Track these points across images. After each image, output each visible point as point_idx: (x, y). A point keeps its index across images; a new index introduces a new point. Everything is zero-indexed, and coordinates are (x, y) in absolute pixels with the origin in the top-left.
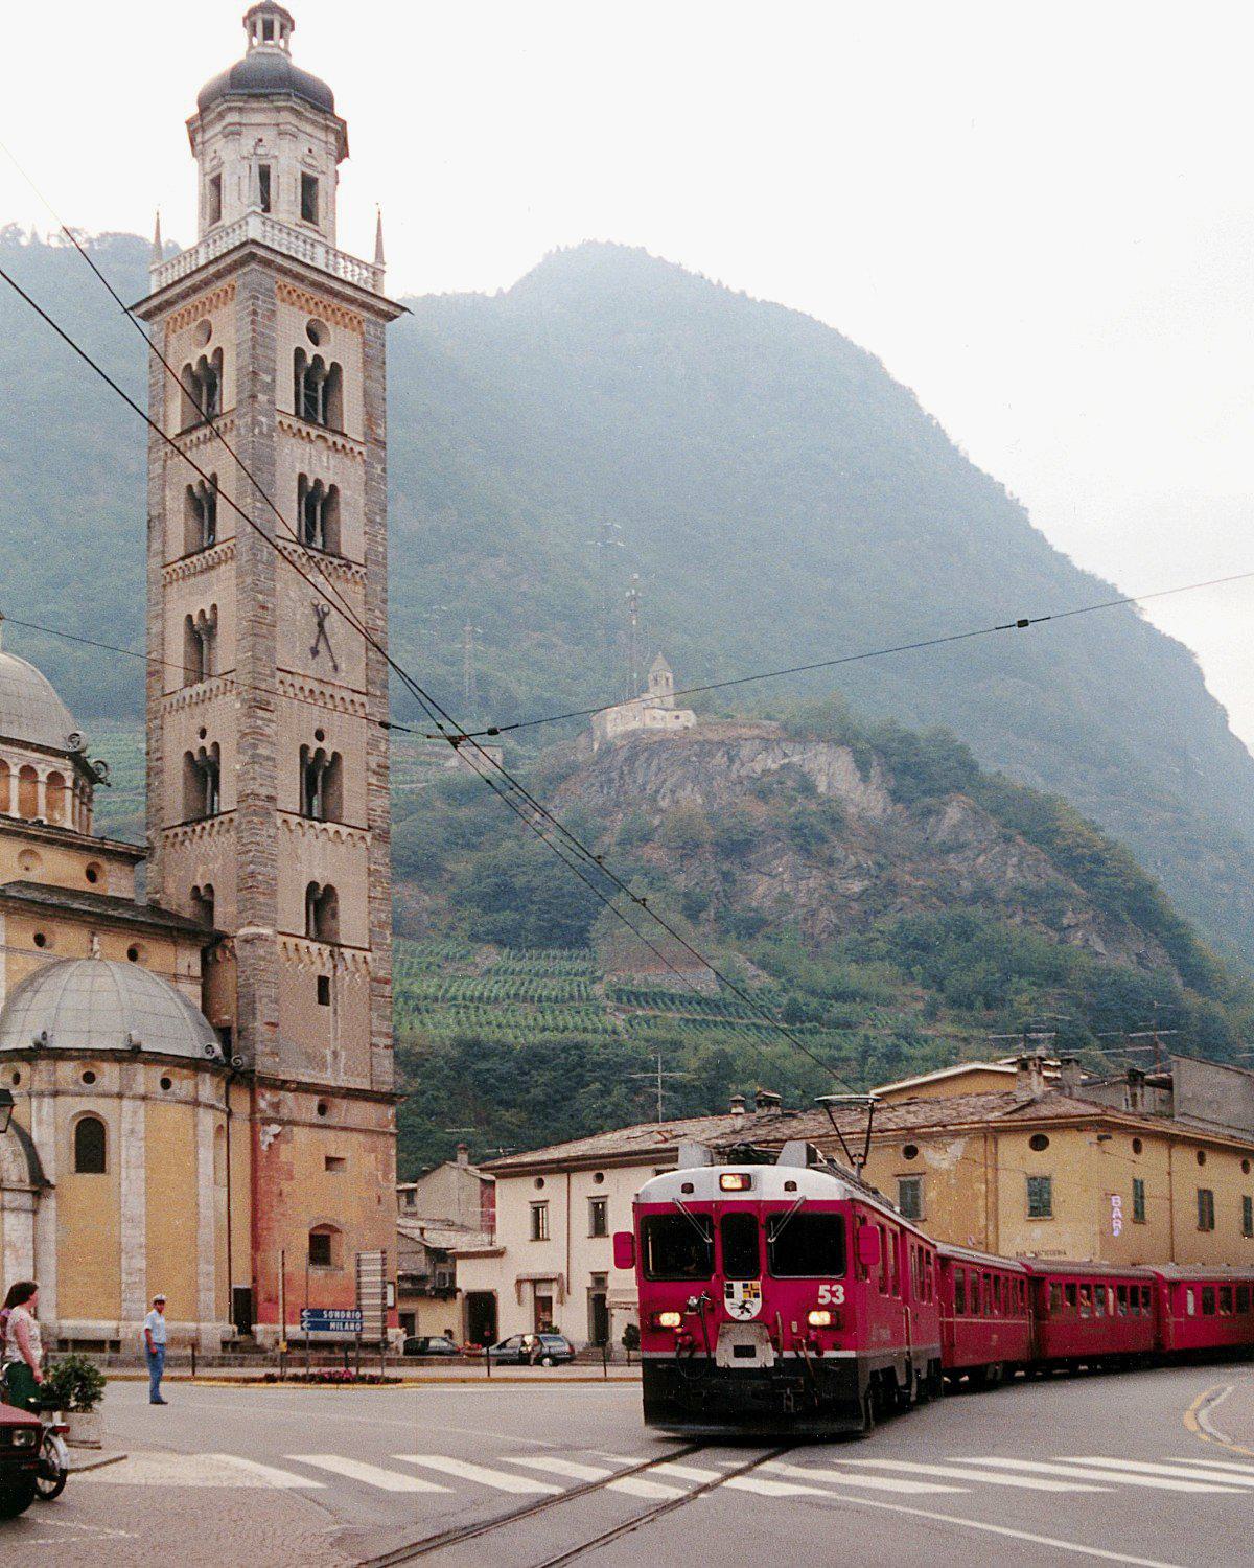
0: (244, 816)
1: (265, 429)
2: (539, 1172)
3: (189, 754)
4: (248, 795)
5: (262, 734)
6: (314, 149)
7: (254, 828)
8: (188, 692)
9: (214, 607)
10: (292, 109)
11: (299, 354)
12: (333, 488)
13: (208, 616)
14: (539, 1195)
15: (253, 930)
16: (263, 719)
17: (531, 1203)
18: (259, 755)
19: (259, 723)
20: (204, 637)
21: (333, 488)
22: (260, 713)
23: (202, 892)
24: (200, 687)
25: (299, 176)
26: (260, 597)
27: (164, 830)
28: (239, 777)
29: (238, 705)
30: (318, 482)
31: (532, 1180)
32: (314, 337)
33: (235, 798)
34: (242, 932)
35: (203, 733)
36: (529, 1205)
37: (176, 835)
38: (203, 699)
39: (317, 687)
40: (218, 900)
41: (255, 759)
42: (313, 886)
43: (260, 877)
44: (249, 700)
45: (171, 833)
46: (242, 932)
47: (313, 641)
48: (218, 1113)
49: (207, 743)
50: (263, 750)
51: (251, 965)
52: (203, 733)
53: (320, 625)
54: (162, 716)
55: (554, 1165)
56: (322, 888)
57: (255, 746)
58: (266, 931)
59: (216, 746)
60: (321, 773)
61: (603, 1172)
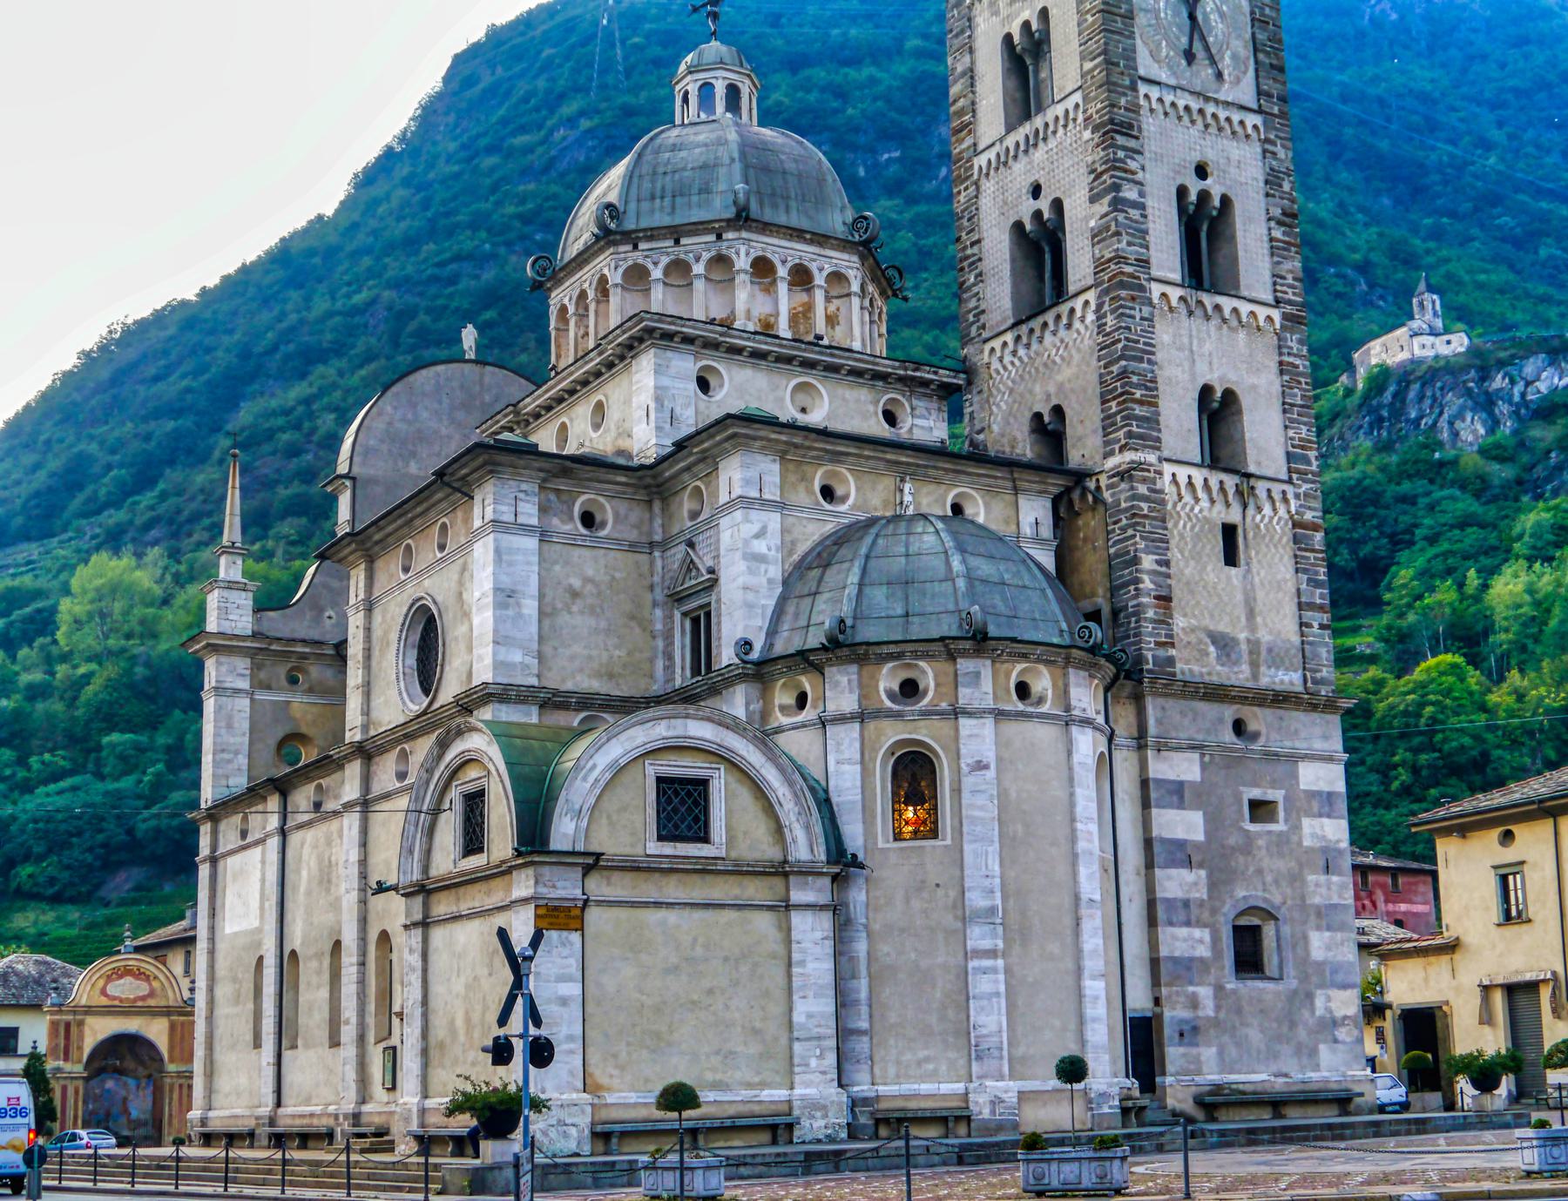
0: (1106, 292)
2: (1505, 822)
3: (1018, 226)
4: (1110, 260)
5: (1126, 171)
7: (1121, 306)
8: (1010, 142)
9: (1044, 14)
13: (1034, 27)
14: (1509, 855)
15: (1129, 456)
16: (1124, 148)
17: (1495, 867)
18: (1125, 201)
19: (1121, 154)
20: (1028, 61)
22: (1121, 140)
23: (1047, 419)
24: (1026, 129)
27: (986, 341)
28: (1098, 236)
29: (1087, 135)
31: (1495, 833)
33: (1091, 270)
34: (1111, 463)
35: (1036, 191)
36: (1493, 872)
37: (1005, 344)
38: (1031, 144)
39: (1195, 105)
40: (1072, 430)
41: (1118, 204)
42: (1206, 391)
43: (1135, 379)
44: (1103, 125)
45: (997, 343)
46: (1111, 463)
47: (1184, 40)
48: (1098, 734)
49: (1044, 204)
50: (1130, 193)
51: (1126, 510)
52: (1036, 191)
53: (1192, 17)
54: (976, 183)
55: (1535, 806)
56: (1219, 394)
57: (1116, 188)
58: (1152, 458)
59: (1058, 205)
60: (1205, 227)
61: (1513, 828)
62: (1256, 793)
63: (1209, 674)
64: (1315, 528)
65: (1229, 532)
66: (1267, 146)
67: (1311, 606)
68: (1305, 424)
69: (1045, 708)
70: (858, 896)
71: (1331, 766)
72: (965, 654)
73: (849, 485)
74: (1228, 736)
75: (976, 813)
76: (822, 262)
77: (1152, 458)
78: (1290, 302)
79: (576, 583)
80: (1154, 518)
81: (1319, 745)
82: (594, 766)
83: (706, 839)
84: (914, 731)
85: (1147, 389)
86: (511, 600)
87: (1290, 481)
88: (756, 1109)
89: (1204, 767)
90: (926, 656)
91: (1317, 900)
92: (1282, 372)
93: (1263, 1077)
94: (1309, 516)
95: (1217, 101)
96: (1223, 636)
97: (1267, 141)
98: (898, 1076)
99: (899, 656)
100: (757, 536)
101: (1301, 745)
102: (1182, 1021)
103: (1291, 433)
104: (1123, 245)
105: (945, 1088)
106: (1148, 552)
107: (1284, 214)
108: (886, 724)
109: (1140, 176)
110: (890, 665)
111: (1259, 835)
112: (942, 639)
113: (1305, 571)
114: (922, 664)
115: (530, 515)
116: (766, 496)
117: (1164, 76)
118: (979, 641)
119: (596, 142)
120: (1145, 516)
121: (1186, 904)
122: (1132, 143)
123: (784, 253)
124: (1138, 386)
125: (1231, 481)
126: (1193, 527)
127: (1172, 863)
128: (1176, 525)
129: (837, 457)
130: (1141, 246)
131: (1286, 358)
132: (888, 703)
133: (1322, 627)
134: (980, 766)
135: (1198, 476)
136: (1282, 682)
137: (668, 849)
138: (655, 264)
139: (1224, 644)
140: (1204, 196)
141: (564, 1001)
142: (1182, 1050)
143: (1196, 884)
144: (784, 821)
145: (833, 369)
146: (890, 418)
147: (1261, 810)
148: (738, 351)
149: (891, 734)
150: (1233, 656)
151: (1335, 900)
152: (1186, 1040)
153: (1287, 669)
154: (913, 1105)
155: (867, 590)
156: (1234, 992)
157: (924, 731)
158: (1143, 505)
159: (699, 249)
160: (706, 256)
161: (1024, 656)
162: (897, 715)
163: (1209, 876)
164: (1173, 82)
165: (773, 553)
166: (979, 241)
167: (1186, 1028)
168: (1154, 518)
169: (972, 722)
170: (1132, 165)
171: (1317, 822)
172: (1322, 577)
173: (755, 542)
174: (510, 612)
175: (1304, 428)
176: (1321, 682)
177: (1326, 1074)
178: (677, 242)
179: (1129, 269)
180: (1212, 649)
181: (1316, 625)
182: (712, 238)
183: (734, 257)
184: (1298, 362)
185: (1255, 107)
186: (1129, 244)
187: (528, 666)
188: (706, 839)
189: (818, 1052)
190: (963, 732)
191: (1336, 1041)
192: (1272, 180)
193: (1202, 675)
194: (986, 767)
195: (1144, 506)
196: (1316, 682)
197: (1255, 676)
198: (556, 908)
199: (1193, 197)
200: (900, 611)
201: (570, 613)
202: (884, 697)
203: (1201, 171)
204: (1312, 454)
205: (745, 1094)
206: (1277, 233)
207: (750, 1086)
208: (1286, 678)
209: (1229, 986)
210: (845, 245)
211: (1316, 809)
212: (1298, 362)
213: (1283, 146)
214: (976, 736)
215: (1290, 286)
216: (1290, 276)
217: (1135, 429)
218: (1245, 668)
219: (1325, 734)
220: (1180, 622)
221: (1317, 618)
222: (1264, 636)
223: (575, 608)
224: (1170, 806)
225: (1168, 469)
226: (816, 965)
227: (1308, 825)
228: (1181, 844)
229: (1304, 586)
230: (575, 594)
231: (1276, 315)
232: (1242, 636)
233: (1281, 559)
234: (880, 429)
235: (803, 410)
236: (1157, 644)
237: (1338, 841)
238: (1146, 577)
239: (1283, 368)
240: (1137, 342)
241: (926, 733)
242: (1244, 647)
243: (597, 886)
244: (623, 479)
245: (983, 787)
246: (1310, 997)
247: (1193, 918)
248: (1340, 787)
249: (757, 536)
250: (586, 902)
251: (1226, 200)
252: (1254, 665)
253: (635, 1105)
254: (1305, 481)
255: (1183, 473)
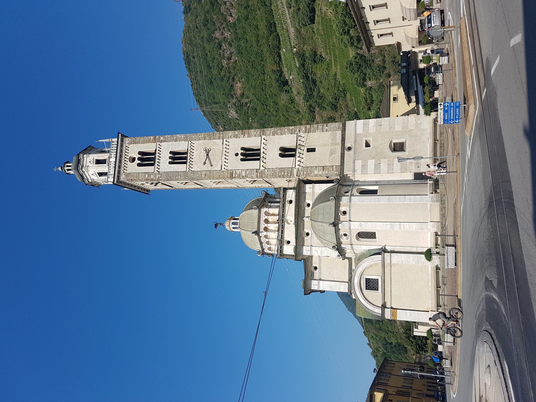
1: (160, 176)
6: (89, 161)
10: (81, 169)
11: (139, 165)
12: (171, 153)
16: (235, 175)
19: (236, 176)
21: (171, 153)
22: (234, 176)
25: (97, 165)
26: (203, 176)
30: (170, 158)
32: (133, 160)
42: (281, 156)
43: (280, 174)
57: (243, 177)
62: (364, 145)
63: (338, 157)
64: (306, 128)
65: (309, 150)
66: (230, 137)
67: (323, 129)
68: (285, 130)
69: (348, 209)
70: (388, 248)
71: (357, 124)
72: (338, 227)
73: (306, 231)
74: (352, 152)
75: (370, 226)
76: (263, 217)
77: (295, 171)
78: (260, 133)
79: (328, 273)
80: (307, 170)
81: (353, 128)
82: (364, 304)
83: (378, 280)
84: (354, 236)
85: (281, 171)
86: (332, 287)
87: (297, 134)
88: (433, 274)
89: (359, 160)
90: (339, 234)
91: (388, 128)
92: (274, 135)
93: (429, 144)
94: (304, 129)
95: (222, 151)
96: (330, 153)
97: (228, 138)
98: (426, 243)
99: (339, 238)
100: (317, 252)
101: (353, 133)
102: (415, 165)
103: (287, 134)
104: (254, 176)
105: (429, 235)
106: (314, 172)
107: (242, 134)
108: (352, 241)
109: (240, 171)
110: (341, 239)
111: (373, 144)
112: (335, 233)
113: (315, 131)
114: (340, 234)
115: (316, 282)
116: (310, 250)
117: (220, 163)
118: (335, 224)
119: (231, 110)
120: (307, 173)
121: (389, 165)
122: (234, 172)
123: (263, 225)
124: (281, 174)
125: (298, 151)
126: (308, 160)
127: (380, 168)
128: (308, 165)
129: (301, 234)
130: (254, 171)
131: (272, 134)
132: (349, 240)
133: (327, 126)
134: (361, 225)
135: (298, 159)
136: (339, 137)
137: (380, 288)
138: (267, 246)
139: (332, 153)
140: (242, 154)
141: (411, 315)
142: (422, 167)
143: (384, 162)
144: (373, 263)
145: (283, 215)
146: (291, 202)
147: (367, 145)
148: (282, 236)
149: (354, 240)
150: (334, 150)
151: (388, 123)
152: (419, 166)
153: (336, 135)
154: (433, 241)
155: (326, 239)
156: (409, 152)
157: (354, 234)
158: (305, 173)
159: (263, 240)
160: (265, 239)
161: (338, 214)
162: (351, 239)
163: (382, 158)
164: (220, 161)
165: (320, 249)
166: (255, 186)
167: (417, 166)
168: (307, 170)
169: (352, 226)
170: (238, 173)
171: (370, 129)
172: (316, 126)
173: (318, 253)
174: (334, 287)
175: (286, 130)
176: (339, 126)
177: (428, 127)
178: (263, 243)
179: (258, 174)
180: (333, 156)
181: (327, 128)
182: (261, 238)
183: (264, 235)
184: (272, 131)
185: (222, 140)
186: (254, 174)
187: (344, 285)
188: (378, 280)
189: (421, 259)
190: (354, 228)
191: (421, 123)
192: (236, 136)
193: (339, 158)
194: (361, 224)
195: (305, 173)
196: (339, 128)
197: (339, 144)
198: (393, 315)
199: (242, 157)
200: (330, 235)
201: (333, 274)
202: (347, 240)
203: (237, 155)
204: (291, 128)
205: (430, 276)
206: (247, 135)
207: (428, 275)
208: (338, 136)
209: (407, 154)
210: (260, 212)
211: (367, 128)
212: (272, 131)
213: (229, 134)
214: (354, 225)
215: (257, 133)
216: (255, 133)
217: (290, 175)
218: (337, 147)
219: (350, 124)
220: (328, 164)
221: (325, 128)
222: (330, 141)
223: (333, 273)
224: (367, 168)
225: (297, 167)
226: (403, 258)
227: (370, 131)
228: (375, 166)
229: (318, 131)
230: (330, 273)
231: (263, 137)
232: (330, 148)
233: (313, 136)
234: (293, 204)
235: (291, 221)
236: (333, 171)
237: (374, 122)
238: (319, 173)
239: (273, 135)
240: (272, 173)
241: (354, 234)
242: (332, 147)
243: (388, 305)
244: (308, 263)
245: (365, 225)
246: (410, 130)
247: (392, 163)
248: (362, 121)
249: (317, 252)
250: (392, 308)
251: (243, 149)
252: (336, 144)
253: (432, 301)
254: (296, 131)
255: (298, 163)
